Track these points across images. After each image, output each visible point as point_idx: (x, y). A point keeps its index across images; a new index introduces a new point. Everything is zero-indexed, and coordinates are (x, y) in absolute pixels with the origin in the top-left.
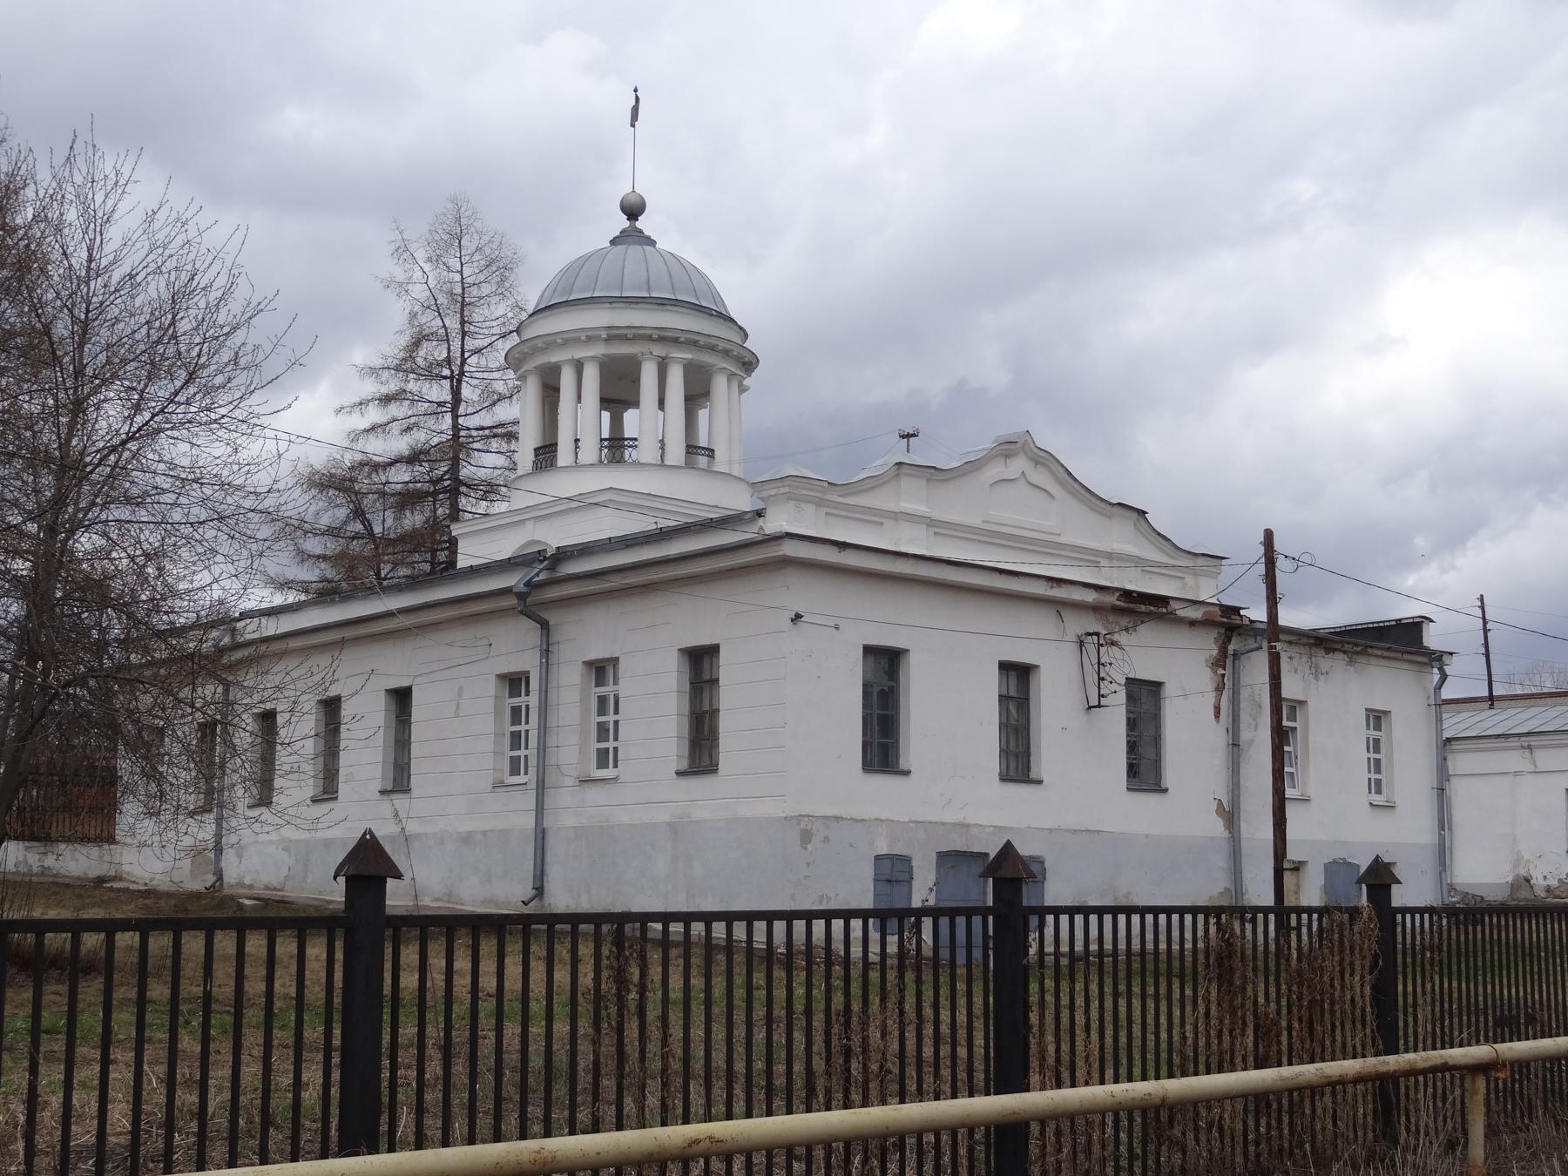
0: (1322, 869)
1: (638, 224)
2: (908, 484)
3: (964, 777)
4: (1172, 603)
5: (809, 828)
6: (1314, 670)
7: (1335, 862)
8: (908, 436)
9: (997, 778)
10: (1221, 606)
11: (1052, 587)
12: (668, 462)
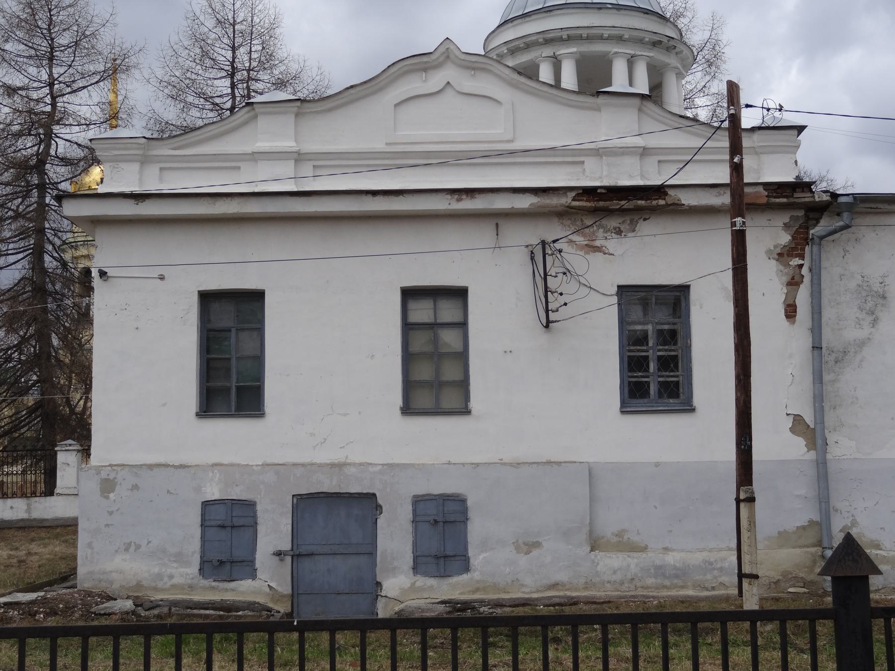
2: (263, 122)
4: (671, 192)
5: (111, 477)
9: (399, 412)
10: (766, 185)
11: (459, 200)
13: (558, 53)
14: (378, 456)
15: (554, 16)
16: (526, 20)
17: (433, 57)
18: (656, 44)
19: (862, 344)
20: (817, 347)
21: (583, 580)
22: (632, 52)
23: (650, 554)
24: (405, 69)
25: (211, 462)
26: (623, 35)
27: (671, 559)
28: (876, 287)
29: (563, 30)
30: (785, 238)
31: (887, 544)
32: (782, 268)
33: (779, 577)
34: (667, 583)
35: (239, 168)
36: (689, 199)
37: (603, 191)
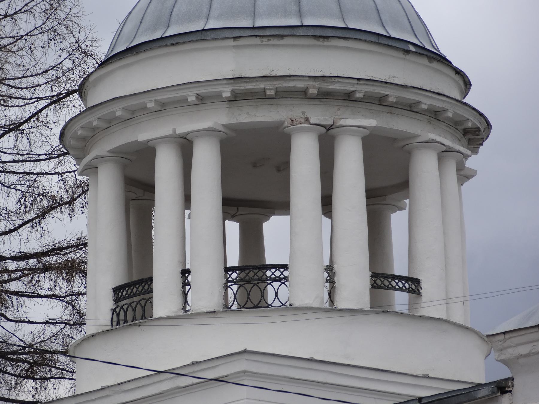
12: (341, 303)
15: (328, 47)
16: (270, 43)
26: (447, 110)
29: (361, 82)
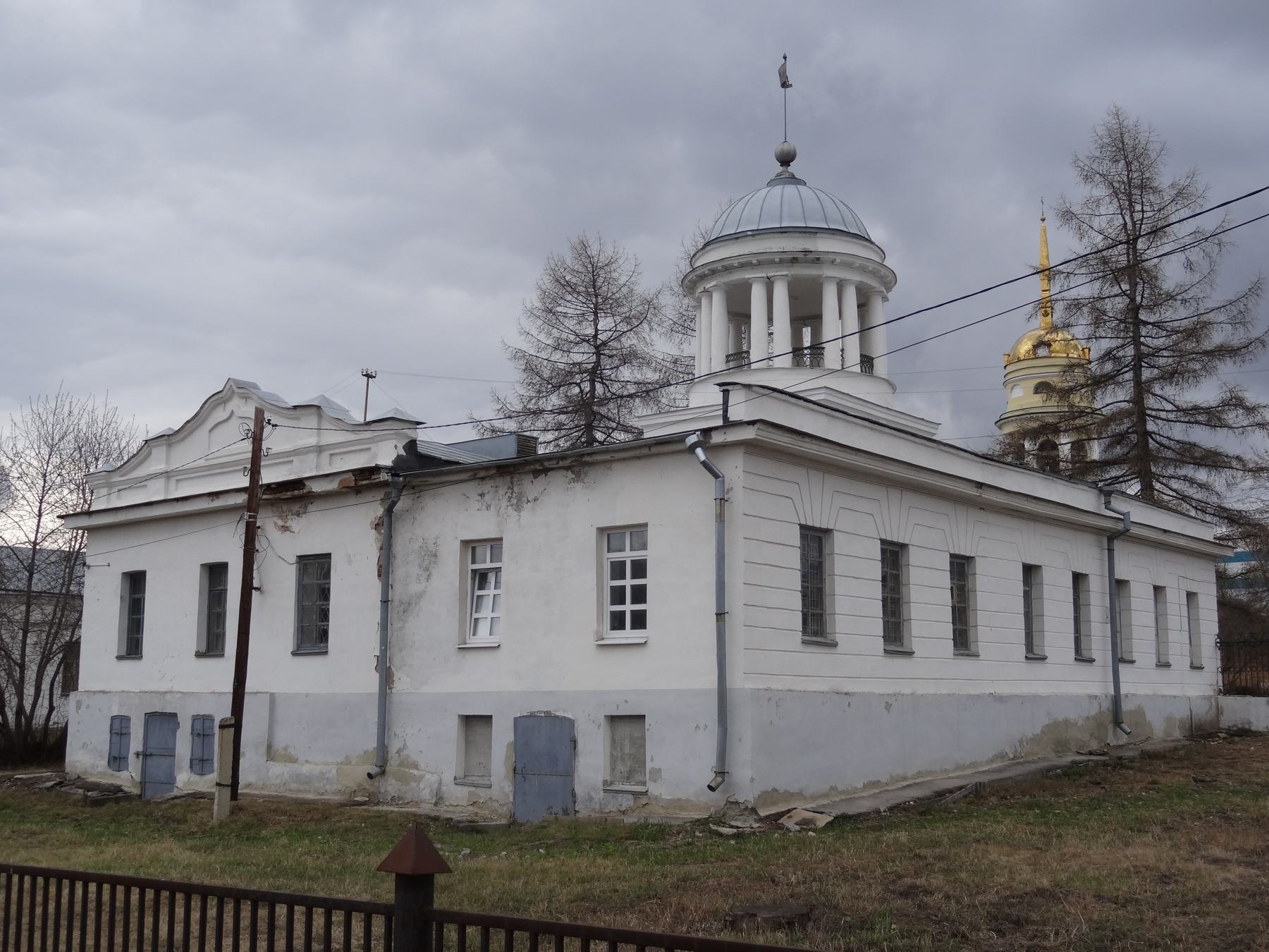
0: (511, 724)
1: (790, 169)
3: (173, 657)
4: (307, 483)
6: (515, 501)
7: (532, 716)
8: (369, 376)
10: (353, 471)
11: (212, 501)
13: (706, 288)
14: (180, 686)
15: (707, 252)
17: (224, 393)
18: (794, 261)
19: (420, 596)
20: (385, 602)
21: (261, 783)
22: (765, 275)
23: (296, 765)
24: (214, 403)
25: (121, 689)
27: (306, 769)
28: (432, 548)
30: (380, 511)
31: (422, 766)
32: (378, 535)
33: (356, 788)
34: (302, 788)
35: (146, 486)
36: (317, 487)
37: (274, 486)
